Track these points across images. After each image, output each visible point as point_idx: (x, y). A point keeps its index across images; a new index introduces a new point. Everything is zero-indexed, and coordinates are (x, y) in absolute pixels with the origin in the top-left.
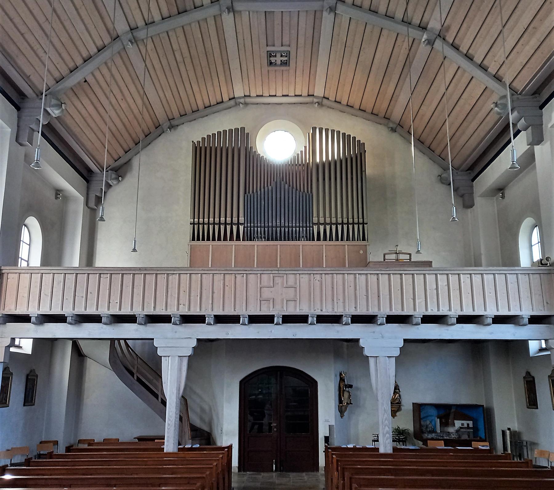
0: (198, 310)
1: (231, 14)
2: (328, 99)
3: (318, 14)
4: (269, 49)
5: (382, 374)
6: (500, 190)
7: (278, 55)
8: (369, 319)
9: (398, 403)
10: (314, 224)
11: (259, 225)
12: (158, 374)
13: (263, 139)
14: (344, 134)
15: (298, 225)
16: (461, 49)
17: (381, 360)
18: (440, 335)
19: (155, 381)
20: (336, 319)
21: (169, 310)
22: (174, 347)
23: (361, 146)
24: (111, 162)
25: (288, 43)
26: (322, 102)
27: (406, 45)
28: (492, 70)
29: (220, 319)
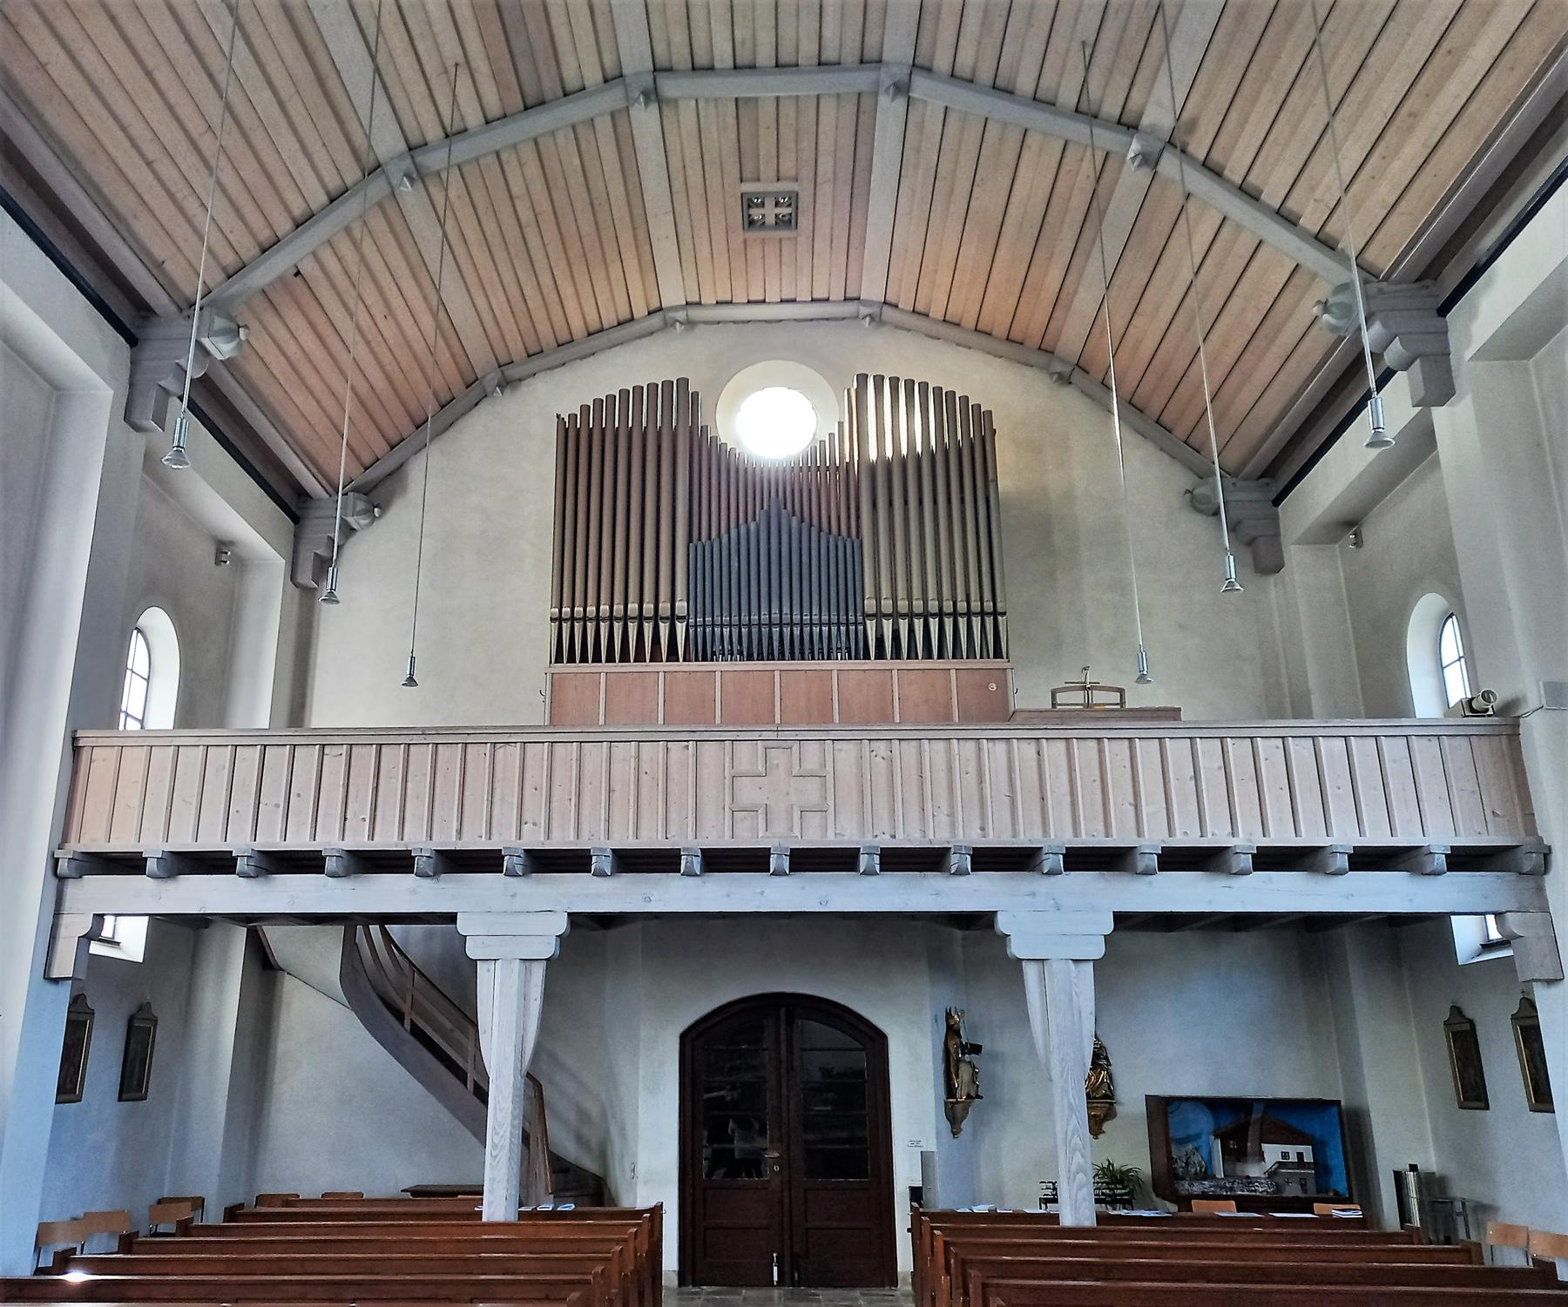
0: (572, 837)
1: (654, 108)
2: (896, 306)
3: (866, 103)
4: (749, 187)
5: (1060, 1010)
6: (1348, 525)
7: (770, 203)
8: (1019, 860)
9: (1105, 1096)
10: (866, 616)
11: (726, 619)
12: (467, 1018)
13: (734, 406)
14: (938, 391)
15: (825, 618)
16: (1226, 173)
17: (1056, 969)
18: (1210, 902)
19: (457, 1034)
20: (930, 860)
21: (495, 837)
22: (509, 935)
23: (983, 419)
24: (357, 470)
25: (792, 173)
26: (881, 315)
27: (1087, 169)
28: (1310, 222)
29: (630, 861)
